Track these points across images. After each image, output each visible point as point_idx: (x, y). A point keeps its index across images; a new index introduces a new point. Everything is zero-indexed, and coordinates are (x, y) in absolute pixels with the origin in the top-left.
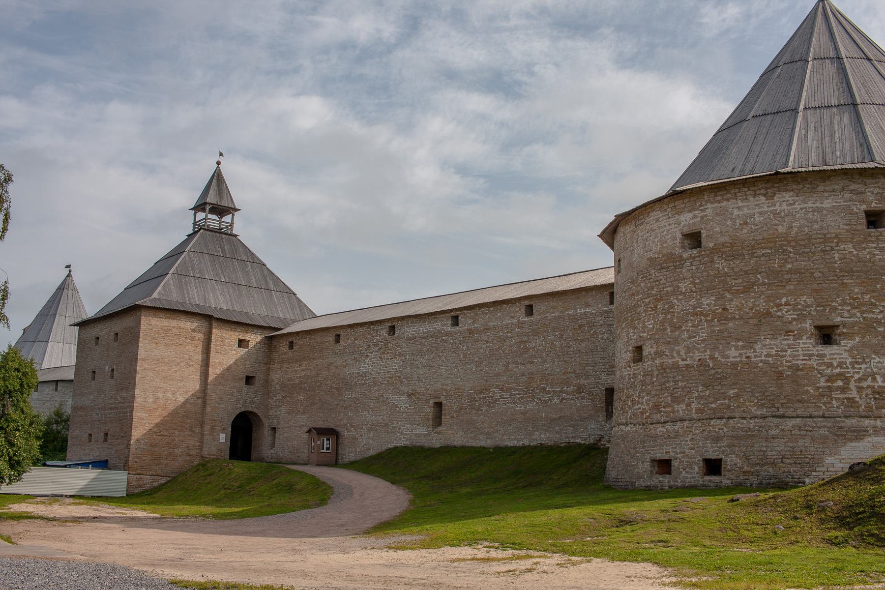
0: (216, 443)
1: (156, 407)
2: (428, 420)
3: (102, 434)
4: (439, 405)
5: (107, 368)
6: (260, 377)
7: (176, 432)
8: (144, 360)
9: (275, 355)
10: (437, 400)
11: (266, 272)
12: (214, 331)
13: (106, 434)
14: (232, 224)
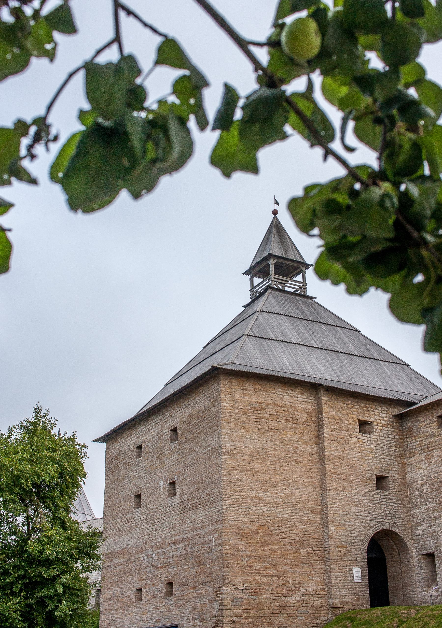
0: (350, 583)
1: (254, 528)
3: (162, 586)
5: (161, 483)
6: (394, 476)
7: (288, 568)
8: (231, 454)
11: (362, 339)
13: (170, 584)
14: (304, 283)
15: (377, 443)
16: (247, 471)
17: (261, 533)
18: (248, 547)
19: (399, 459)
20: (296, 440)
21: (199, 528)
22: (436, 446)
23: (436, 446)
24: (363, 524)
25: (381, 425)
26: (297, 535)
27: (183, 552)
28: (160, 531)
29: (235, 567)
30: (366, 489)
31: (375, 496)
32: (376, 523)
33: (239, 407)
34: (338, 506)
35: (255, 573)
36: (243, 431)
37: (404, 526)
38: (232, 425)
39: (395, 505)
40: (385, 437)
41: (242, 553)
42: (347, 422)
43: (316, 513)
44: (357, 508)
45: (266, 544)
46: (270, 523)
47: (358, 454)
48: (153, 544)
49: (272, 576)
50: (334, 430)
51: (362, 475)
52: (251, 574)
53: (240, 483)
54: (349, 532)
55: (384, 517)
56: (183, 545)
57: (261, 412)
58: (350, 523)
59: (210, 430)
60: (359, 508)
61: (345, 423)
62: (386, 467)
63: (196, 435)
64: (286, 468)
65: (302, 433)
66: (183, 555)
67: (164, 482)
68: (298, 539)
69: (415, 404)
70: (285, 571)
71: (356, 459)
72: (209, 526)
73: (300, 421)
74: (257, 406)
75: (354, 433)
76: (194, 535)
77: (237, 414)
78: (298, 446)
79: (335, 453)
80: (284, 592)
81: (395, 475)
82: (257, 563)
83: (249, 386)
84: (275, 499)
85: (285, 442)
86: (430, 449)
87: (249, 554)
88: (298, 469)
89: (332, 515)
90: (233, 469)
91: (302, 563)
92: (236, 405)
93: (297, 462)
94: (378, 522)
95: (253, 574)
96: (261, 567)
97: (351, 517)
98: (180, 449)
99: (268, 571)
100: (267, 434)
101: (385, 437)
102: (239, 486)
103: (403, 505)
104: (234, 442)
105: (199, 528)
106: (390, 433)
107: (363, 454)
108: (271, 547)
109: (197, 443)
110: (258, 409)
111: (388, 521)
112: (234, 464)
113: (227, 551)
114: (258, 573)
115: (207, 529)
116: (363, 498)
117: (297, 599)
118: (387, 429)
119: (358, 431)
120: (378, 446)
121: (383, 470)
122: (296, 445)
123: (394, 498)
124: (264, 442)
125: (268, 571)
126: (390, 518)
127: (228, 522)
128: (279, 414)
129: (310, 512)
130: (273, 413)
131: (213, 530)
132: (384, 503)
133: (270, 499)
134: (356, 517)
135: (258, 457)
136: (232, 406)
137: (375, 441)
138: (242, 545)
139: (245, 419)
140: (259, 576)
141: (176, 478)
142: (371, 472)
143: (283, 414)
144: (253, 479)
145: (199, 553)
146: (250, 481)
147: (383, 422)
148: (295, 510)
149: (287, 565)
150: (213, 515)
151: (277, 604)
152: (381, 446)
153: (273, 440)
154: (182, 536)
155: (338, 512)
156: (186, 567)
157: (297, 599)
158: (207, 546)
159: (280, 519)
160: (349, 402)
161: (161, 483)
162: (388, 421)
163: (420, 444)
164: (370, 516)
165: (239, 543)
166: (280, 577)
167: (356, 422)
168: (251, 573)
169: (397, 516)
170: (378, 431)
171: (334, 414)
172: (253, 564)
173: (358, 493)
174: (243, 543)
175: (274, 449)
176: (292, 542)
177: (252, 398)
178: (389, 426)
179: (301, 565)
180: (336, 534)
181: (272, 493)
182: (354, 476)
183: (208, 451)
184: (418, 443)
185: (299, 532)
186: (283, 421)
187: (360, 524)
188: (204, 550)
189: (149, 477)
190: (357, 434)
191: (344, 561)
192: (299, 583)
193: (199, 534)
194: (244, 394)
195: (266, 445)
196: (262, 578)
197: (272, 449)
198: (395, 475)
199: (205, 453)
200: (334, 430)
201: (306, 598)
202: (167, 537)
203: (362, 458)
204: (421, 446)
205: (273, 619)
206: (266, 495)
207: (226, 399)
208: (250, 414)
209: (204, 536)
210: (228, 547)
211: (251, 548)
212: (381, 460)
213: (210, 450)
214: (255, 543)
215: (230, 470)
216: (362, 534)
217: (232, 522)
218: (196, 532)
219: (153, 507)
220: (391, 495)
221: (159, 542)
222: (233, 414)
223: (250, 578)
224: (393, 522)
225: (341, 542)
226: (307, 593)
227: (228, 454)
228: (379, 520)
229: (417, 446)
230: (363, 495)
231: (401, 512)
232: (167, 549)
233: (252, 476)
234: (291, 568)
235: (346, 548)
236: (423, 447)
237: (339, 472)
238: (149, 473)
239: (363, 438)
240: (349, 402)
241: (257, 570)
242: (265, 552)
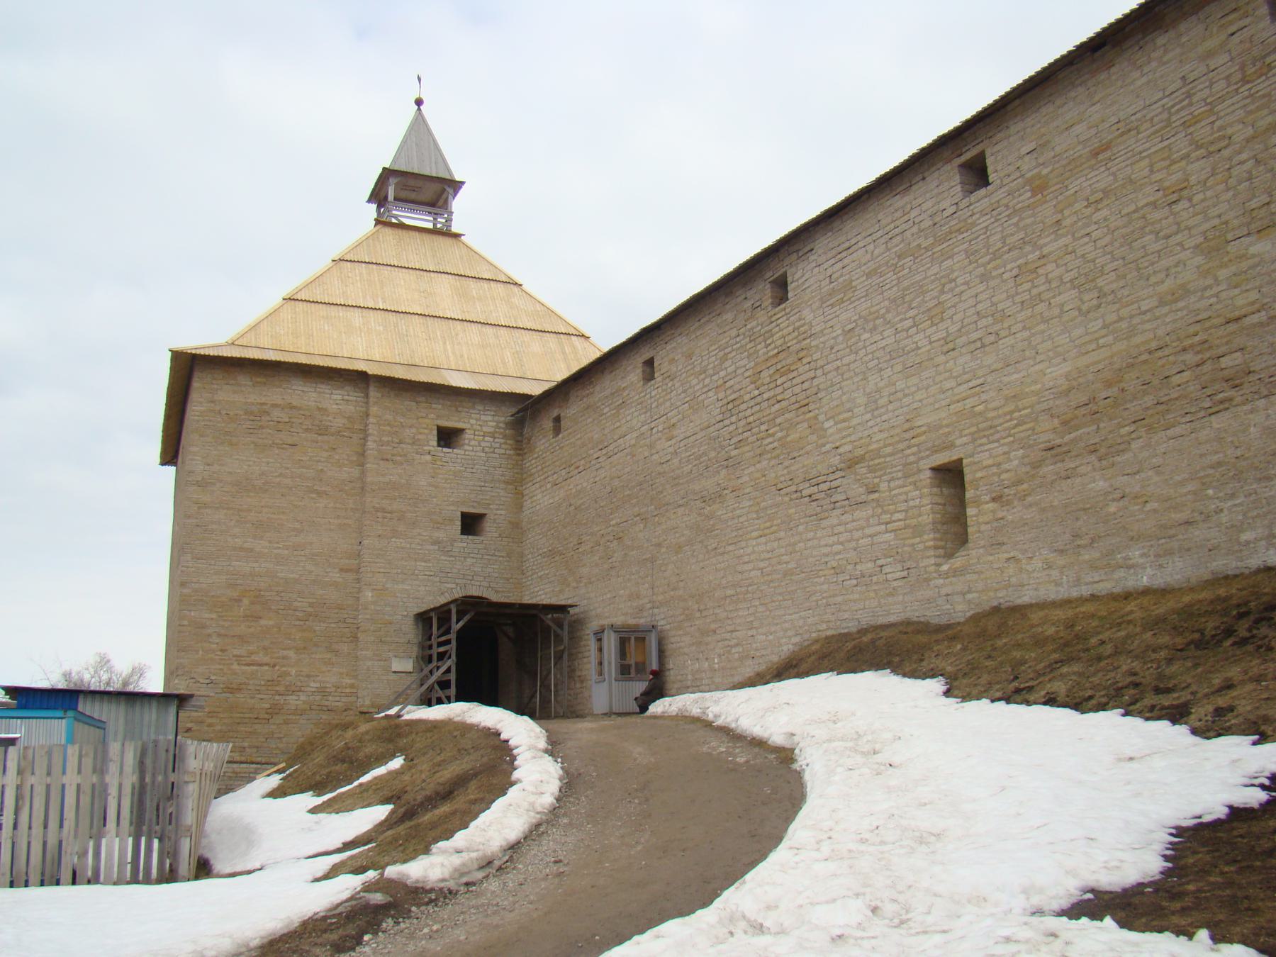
2: (917, 531)
4: (951, 476)
7: (291, 653)
9: (531, 463)
10: (942, 458)
12: (374, 410)
17: (246, 601)
26: (311, 605)
29: (197, 652)
30: (440, 535)
41: (210, 631)
42: (414, 430)
43: (347, 571)
47: (431, 480)
49: (261, 665)
50: (388, 443)
53: (214, 527)
58: (401, 586)
61: (409, 433)
68: (310, 609)
70: (284, 658)
73: (333, 430)
79: (387, 479)
80: (281, 689)
83: (244, 379)
87: (223, 632)
91: (316, 645)
92: (218, 408)
93: (319, 493)
99: (254, 657)
108: (263, 622)
117: (302, 698)
119: (435, 443)
125: (254, 657)
147: (485, 429)
151: (267, 706)
157: (302, 698)
160: (423, 399)
162: (497, 427)
165: (207, 616)
166: (274, 666)
170: (473, 443)
171: (390, 418)
174: (214, 616)
176: (300, 614)
187: (422, 588)
191: (384, 642)
192: (308, 676)
194: (235, 392)
200: (388, 443)
201: (318, 698)
203: (436, 487)
205: (257, 726)
210: (186, 623)
211: (227, 624)
217: (196, 586)
226: (322, 691)
227: (198, 484)
230: (434, 543)
242: (252, 630)
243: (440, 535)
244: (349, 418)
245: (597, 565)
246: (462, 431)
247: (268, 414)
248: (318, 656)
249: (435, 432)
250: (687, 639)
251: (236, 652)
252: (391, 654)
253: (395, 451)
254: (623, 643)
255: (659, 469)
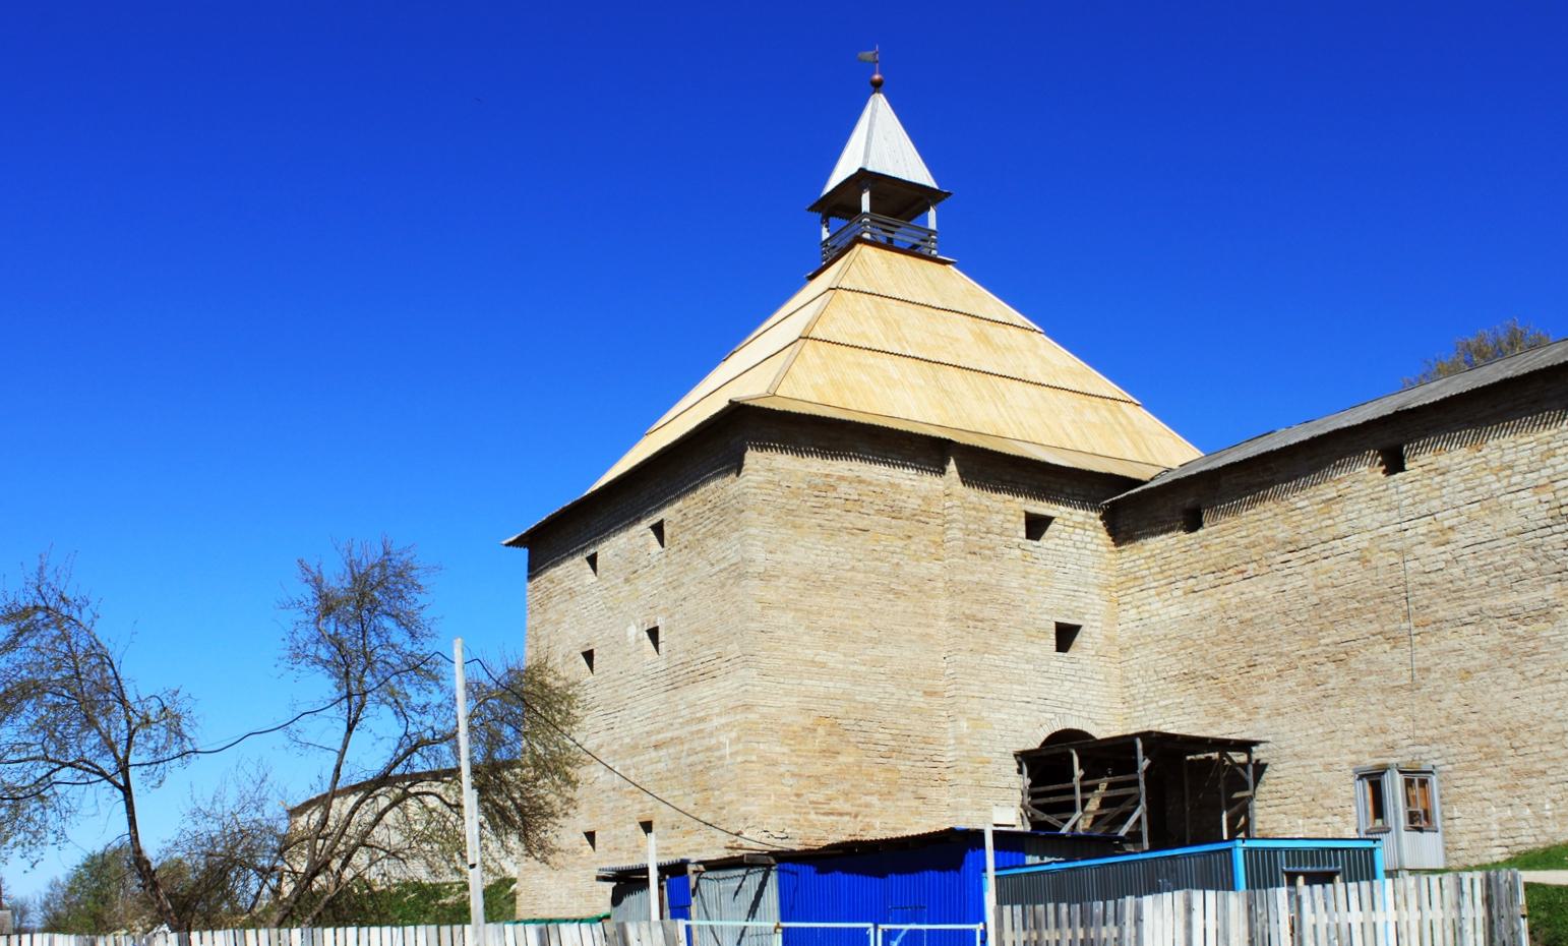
1: (808, 722)
5: (632, 631)
7: (874, 800)
8: (765, 577)
15: (1061, 559)
16: (797, 610)
17: (821, 731)
18: (795, 759)
19: (1105, 593)
20: (898, 550)
21: (702, 720)
22: (1178, 568)
23: (1178, 568)
24: (1026, 718)
25: (1071, 524)
26: (894, 737)
27: (671, 766)
28: (629, 722)
29: (769, 796)
31: (1052, 663)
32: (1052, 716)
33: (784, 484)
34: (977, 683)
35: (806, 807)
36: (790, 532)
37: (1109, 724)
38: (769, 519)
39: (1093, 682)
40: (1078, 548)
41: (782, 769)
42: (1001, 517)
44: (1015, 686)
45: (831, 753)
46: (839, 712)
48: (616, 747)
49: (841, 814)
50: (974, 532)
51: (1026, 623)
52: (798, 810)
53: (781, 633)
54: (996, 732)
55: (1069, 706)
56: (672, 750)
57: (829, 494)
58: (998, 716)
59: (726, 529)
60: (1020, 688)
62: (1077, 607)
63: (699, 537)
64: (876, 606)
65: (909, 537)
66: (669, 771)
67: (637, 627)
68: (893, 743)
69: (1138, 483)
70: (867, 806)
71: (1017, 591)
72: (719, 715)
73: (907, 512)
74: (818, 481)
75: (1015, 540)
76: (692, 733)
77: (780, 497)
78: (902, 563)
79: (975, 578)
81: (1095, 624)
82: (813, 790)
84: (852, 667)
85: (876, 555)
86: (1166, 574)
87: (796, 770)
88: (900, 609)
89: (964, 700)
90: (767, 606)
91: (900, 790)
92: (777, 479)
94: (1056, 714)
95: (804, 810)
96: (820, 797)
97: (1001, 703)
98: (667, 564)
99: (835, 805)
100: (838, 538)
101: (1078, 548)
102: (780, 639)
103: (1108, 682)
104: (771, 552)
105: (702, 720)
106: (1089, 539)
107: (1031, 581)
108: (841, 759)
109: (699, 553)
110: (824, 489)
111: (1077, 713)
112: (771, 596)
113: (753, 765)
114: (814, 808)
115: (716, 722)
116: (1027, 666)
118: (1082, 532)
119: (1024, 534)
120: (1063, 565)
121: (1070, 613)
122: (896, 561)
123: (1090, 668)
124: (833, 554)
126: (1081, 708)
127: (755, 709)
128: (864, 498)
129: (920, 693)
130: (852, 497)
131: (727, 724)
132: (1068, 677)
133: (841, 666)
134: (1012, 704)
135: (819, 584)
136: (770, 482)
137: (1057, 555)
138: (784, 754)
139: (794, 507)
140: (816, 813)
141: (660, 622)
142: (1045, 617)
143: (871, 500)
144: (808, 627)
145: (700, 767)
146: (802, 629)
148: (891, 689)
149: (873, 794)
150: (728, 696)
152: (1069, 566)
153: (851, 550)
154: (669, 735)
155: (976, 694)
156: (676, 793)
158: (717, 754)
159: (861, 706)
161: (632, 631)
163: (1146, 563)
164: (1041, 701)
165: (778, 749)
166: (856, 816)
167: (1020, 517)
168: (801, 807)
169: (1095, 703)
171: (975, 499)
172: (803, 791)
173: (1018, 658)
175: (853, 569)
177: (811, 466)
178: (1087, 527)
179: (899, 795)
180: (970, 736)
181: (845, 655)
182: (1012, 623)
183: (721, 571)
184: (1143, 561)
185: (898, 732)
186: (872, 512)
187: (1020, 718)
188: (710, 762)
189: (609, 618)
190: (1021, 541)
193: (701, 731)
195: (837, 560)
196: (822, 818)
197: (848, 567)
198: (1095, 624)
199: (715, 574)
200: (974, 532)
202: (641, 734)
203: (1028, 590)
204: (1149, 568)
206: (834, 659)
207: (758, 467)
208: (806, 498)
209: (711, 735)
210: (754, 758)
211: (801, 761)
212: (1068, 593)
213: (725, 569)
214: (809, 751)
215: (763, 608)
216: (1022, 737)
218: (695, 728)
219: (616, 676)
220: (1085, 662)
221: (628, 744)
222: (770, 498)
223: (797, 816)
224: (1085, 714)
225: (981, 750)
227: (761, 577)
228: (1057, 710)
229: (1142, 567)
231: (1103, 697)
232: (642, 758)
233: (807, 622)
234: (879, 800)
235: (989, 763)
236: (1152, 571)
237: (980, 616)
238: (611, 609)
239: (1031, 549)
240: (1008, 478)
241: (811, 803)
243: (1034, 650)
244: (924, 499)
245: (1292, 692)
246: (1048, 520)
247: (835, 489)
248: (904, 804)
249: (1023, 520)
250: (1489, 782)
251: (813, 798)
252: (990, 802)
253: (983, 543)
254: (1409, 783)
255: (1424, 579)
